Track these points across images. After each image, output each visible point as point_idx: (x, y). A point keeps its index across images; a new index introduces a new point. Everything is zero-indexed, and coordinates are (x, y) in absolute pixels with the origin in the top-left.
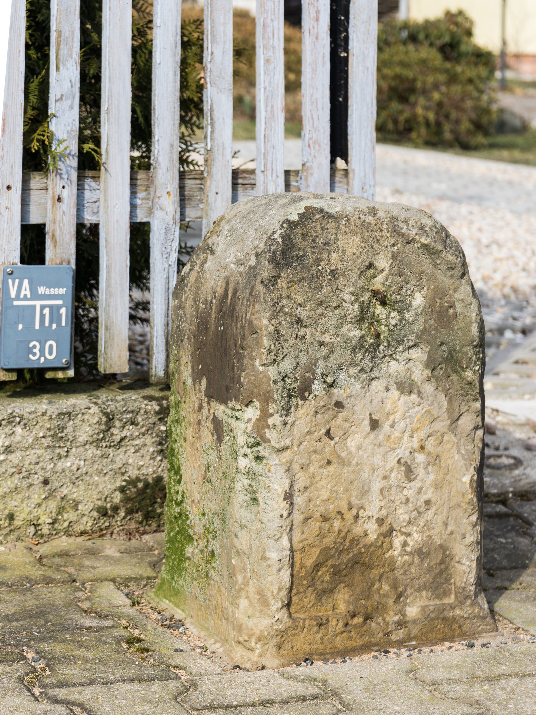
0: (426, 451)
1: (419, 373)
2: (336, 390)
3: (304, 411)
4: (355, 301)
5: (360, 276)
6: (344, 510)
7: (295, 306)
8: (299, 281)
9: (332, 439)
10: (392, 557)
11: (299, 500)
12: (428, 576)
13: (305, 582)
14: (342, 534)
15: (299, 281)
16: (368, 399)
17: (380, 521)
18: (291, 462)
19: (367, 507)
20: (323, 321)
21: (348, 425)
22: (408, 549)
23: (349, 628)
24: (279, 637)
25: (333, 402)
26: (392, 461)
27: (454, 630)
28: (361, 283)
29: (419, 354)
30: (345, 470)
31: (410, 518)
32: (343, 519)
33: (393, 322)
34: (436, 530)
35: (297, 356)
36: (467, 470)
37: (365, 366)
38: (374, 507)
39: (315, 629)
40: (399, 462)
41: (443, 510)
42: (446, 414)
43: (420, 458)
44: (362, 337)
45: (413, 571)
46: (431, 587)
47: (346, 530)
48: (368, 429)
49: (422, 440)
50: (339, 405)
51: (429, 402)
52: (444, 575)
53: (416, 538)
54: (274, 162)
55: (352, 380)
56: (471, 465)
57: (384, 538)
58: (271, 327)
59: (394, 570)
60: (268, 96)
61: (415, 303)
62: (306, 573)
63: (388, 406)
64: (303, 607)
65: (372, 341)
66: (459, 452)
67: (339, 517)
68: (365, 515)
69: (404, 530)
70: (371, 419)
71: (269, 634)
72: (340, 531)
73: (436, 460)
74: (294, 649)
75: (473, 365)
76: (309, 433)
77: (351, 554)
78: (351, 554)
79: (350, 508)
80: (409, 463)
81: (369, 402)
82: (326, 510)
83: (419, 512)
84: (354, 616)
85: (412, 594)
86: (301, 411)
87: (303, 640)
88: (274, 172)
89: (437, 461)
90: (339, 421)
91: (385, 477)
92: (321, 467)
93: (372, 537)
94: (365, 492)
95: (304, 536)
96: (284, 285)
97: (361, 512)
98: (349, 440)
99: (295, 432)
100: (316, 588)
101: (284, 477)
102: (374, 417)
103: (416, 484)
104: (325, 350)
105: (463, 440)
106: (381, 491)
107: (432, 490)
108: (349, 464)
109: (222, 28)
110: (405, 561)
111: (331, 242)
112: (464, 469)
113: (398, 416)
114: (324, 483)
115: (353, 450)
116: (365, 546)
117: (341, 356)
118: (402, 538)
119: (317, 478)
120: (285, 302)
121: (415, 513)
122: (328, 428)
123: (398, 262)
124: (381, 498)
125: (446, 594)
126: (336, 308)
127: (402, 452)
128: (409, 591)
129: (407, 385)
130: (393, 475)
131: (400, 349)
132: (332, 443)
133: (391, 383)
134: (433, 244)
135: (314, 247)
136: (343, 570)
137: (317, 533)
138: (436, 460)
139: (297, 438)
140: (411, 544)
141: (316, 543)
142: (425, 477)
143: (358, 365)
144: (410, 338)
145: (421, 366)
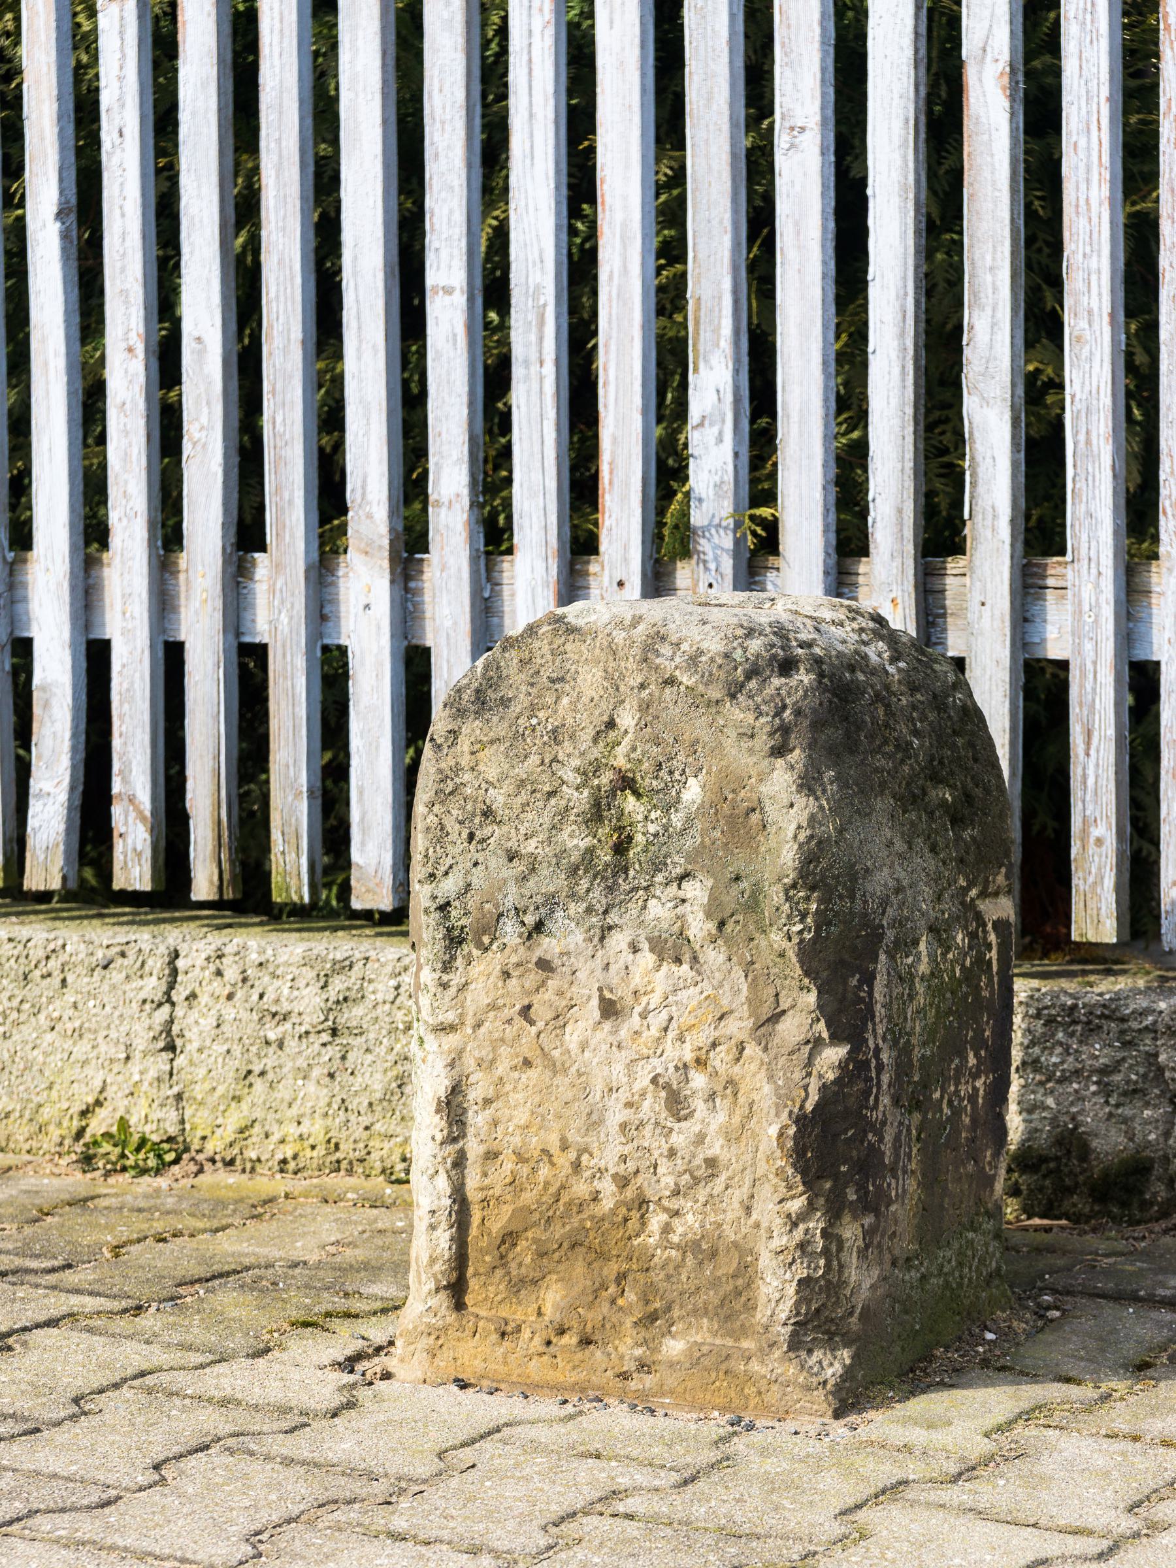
0: (709, 1069)
1: (699, 927)
2: (548, 940)
3: (482, 968)
4: (584, 785)
5: (595, 740)
6: (555, 1149)
7: (484, 786)
8: (492, 742)
9: (532, 1023)
10: (644, 1246)
11: (477, 1120)
12: (712, 1293)
13: (488, 1258)
14: (553, 1190)
15: (492, 742)
16: (599, 961)
17: (623, 1182)
18: (461, 1053)
19: (596, 1152)
20: (530, 816)
21: (564, 1003)
22: (675, 1239)
23: (552, 1349)
24: (433, 1337)
25: (535, 959)
26: (643, 1080)
27: (747, 1398)
28: (595, 753)
29: (696, 891)
30: (558, 1080)
31: (676, 1184)
32: (553, 1164)
33: (652, 828)
34: (730, 1216)
35: (467, 872)
36: (777, 1115)
37: (594, 902)
38: (609, 1153)
39: (494, 1337)
40: (654, 1081)
41: (743, 1179)
42: (745, 1007)
43: (699, 1080)
44: (590, 851)
45: (684, 1278)
46: (717, 1314)
47: (558, 1184)
48: (597, 1014)
49: (700, 1049)
50: (544, 965)
51: (715, 982)
52: (743, 1299)
53: (688, 1224)
54: (1094, 544)
55: (573, 925)
56: (786, 1106)
57: (629, 1210)
58: (431, 817)
59: (647, 1270)
60: (1079, 412)
61: (687, 796)
62: (489, 1244)
63: (637, 980)
64: (485, 1299)
65: (608, 858)
66: (771, 1078)
67: (546, 1159)
68: (592, 1163)
69: (665, 1202)
70: (602, 998)
71: (415, 1328)
72: (547, 1184)
73: (725, 1088)
74: (459, 1362)
75: (784, 921)
76: (493, 1007)
77: (568, 1227)
78: (568, 1227)
79: (565, 1147)
80: (675, 1087)
81: (600, 968)
82: (524, 1144)
83: (693, 1177)
84: (561, 1332)
85: (681, 1318)
86: (477, 969)
87: (473, 1351)
88: (1093, 565)
89: (728, 1091)
90: (548, 995)
91: (629, 1105)
92: (514, 1068)
93: (607, 1204)
94: (594, 1123)
95: (487, 1182)
96: (466, 748)
97: (585, 1158)
98: (568, 1029)
99: (468, 1002)
100: (509, 1273)
101: (443, 1075)
102: (608, 995)
103: (692, 1127)
104: (520, 867)
105: (782, 1061)
106: (624, 1127)
107: (721, 1141)
108: (565, 1071)
109: (989, 278)
110: (669, 1259)
111: (568, 678)
112: (773, 1112)
113: (655, 999)
114: (520, 1096)
115: (574, 1047)
116: (592, 1218)
117: (550, 881)
118: (664, 1217)
119: (508, 1087)
120: (467, 777)
121: (687, 1176)
122: (526, 1002)
123: (650, 718)
124: (623, 1140)
125: (744, 1331)
126: (551, 794)
127: (662, 1064)
128: (676, 1312)
129: (669, 944)
130: (646, 1105)
131: (659, 878)
132: (534, 1030)
133: (642, 939)
134: (701, 688)
135: (532, 685)
136: (554, 1251)
137: (508, 1180)
138: (725, 1088)
139: (471, 1014)
140: (680, 1230)
141: (508, 1197)
142: (709, 1119)
143: (582, 899)
144: (676, 859)
145: (701, 915)
